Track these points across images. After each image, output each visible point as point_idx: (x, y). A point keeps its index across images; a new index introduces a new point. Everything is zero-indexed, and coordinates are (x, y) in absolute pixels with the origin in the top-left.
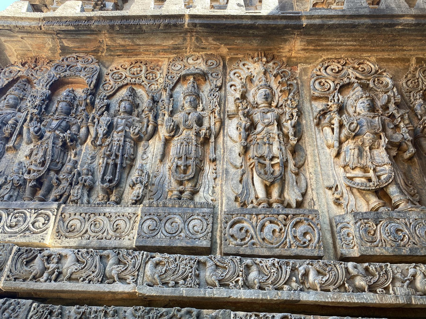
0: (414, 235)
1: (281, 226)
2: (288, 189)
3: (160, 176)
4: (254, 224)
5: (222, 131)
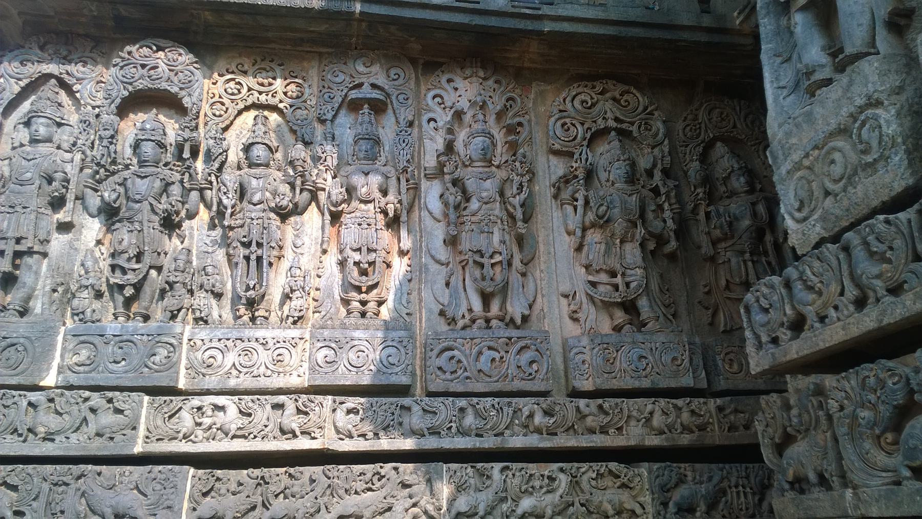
0: (659, 363)
1: (503, 353)
2: (511, 298)
3: (327, 275)
4: (468, 352)
5: (417, 201)
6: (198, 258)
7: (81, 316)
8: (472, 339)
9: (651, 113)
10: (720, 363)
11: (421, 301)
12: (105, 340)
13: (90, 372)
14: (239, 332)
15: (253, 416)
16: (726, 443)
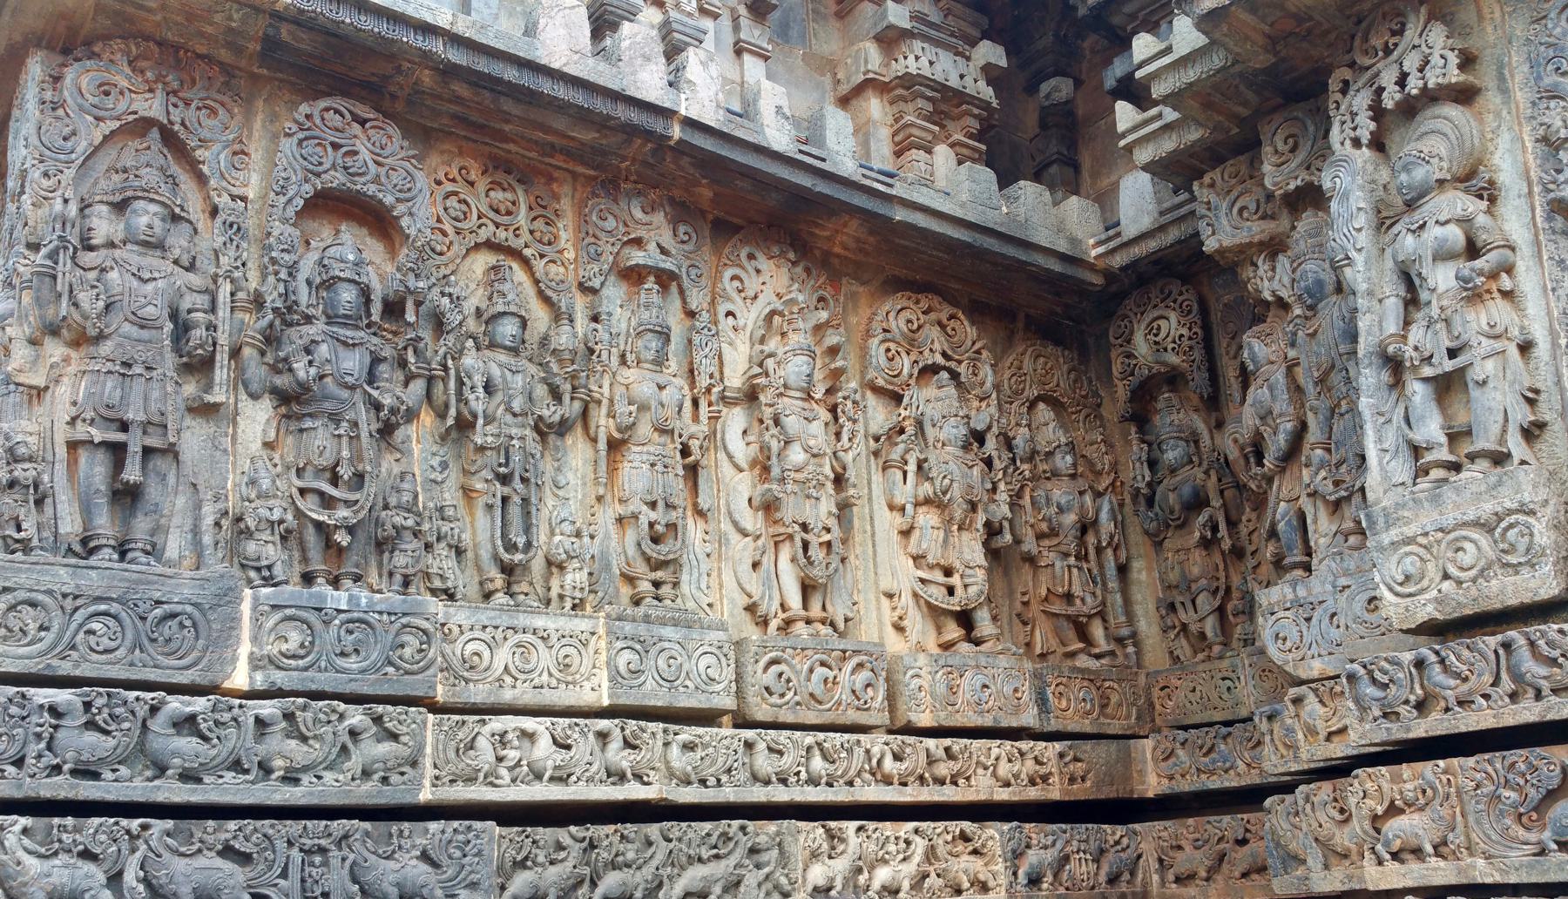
3: (601, 536)
4: (799, 667)
6: (423, 489)
7: (266, 573)
8: (803, 649)
9: (978, 352)
10: (1051, 696)
11: (721, 586)
12: (325, 618)
13: (306, 669)
14: (511, 617)
15: (574, 749)
16: (1067, 799)
